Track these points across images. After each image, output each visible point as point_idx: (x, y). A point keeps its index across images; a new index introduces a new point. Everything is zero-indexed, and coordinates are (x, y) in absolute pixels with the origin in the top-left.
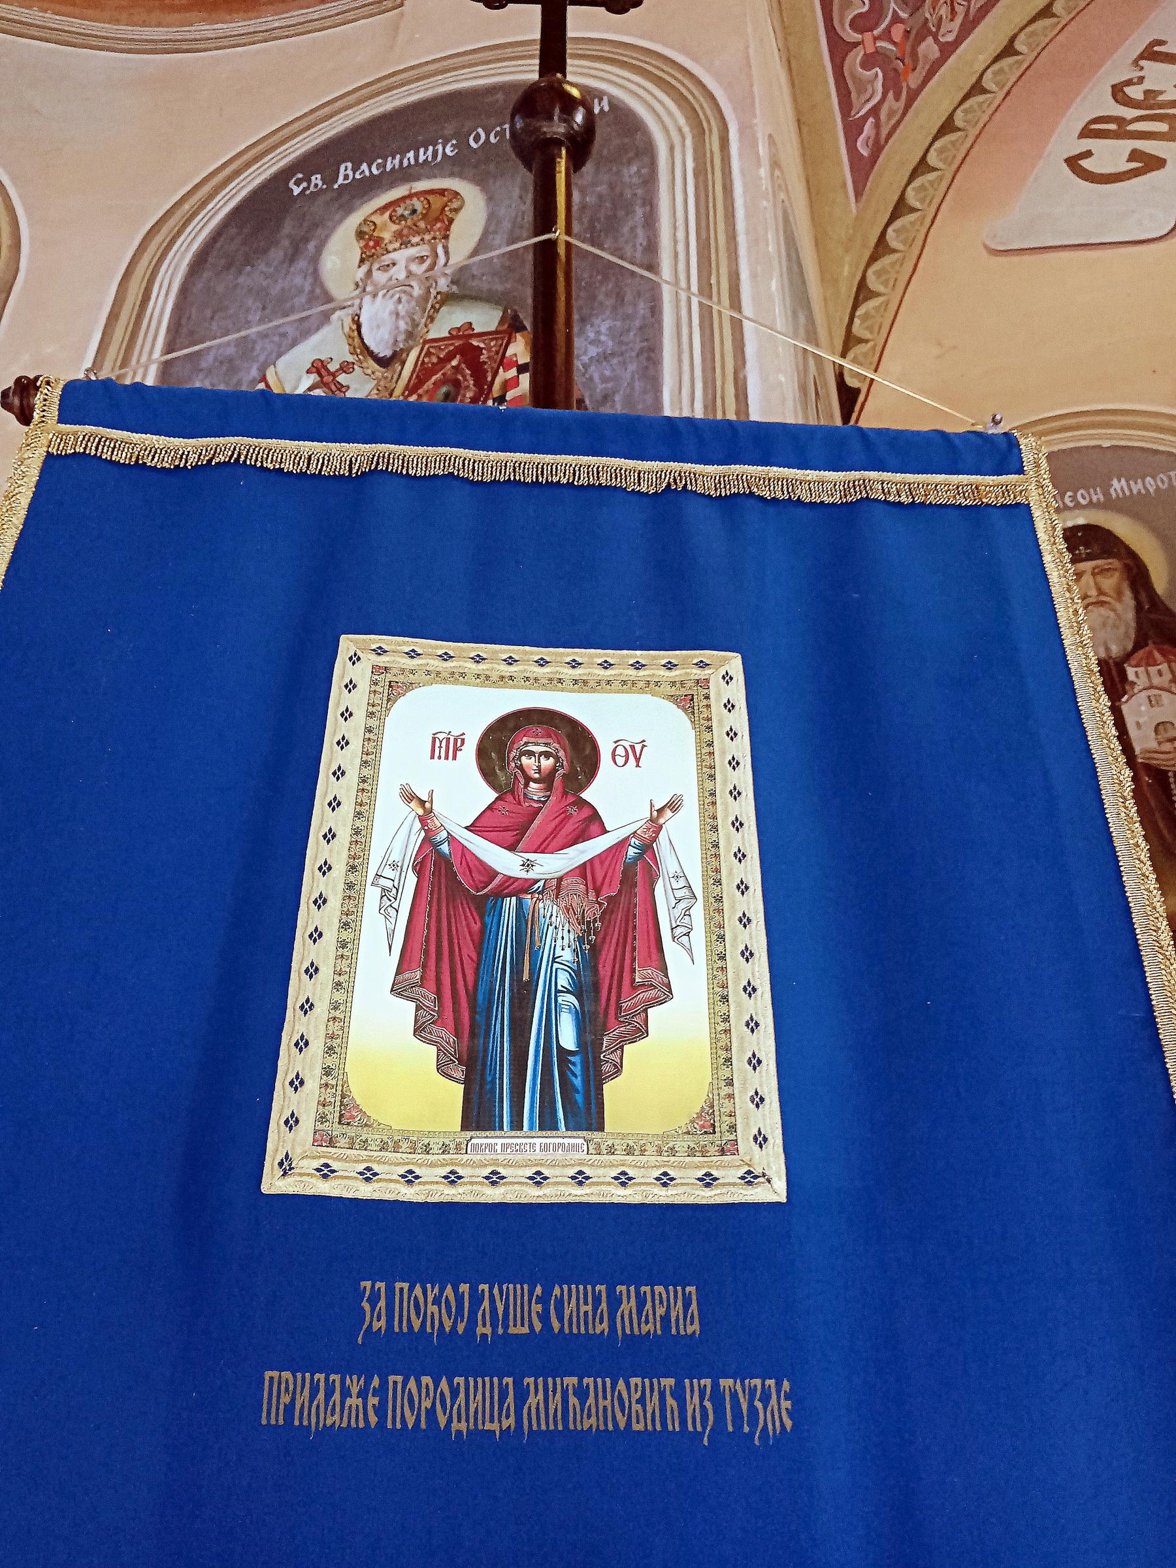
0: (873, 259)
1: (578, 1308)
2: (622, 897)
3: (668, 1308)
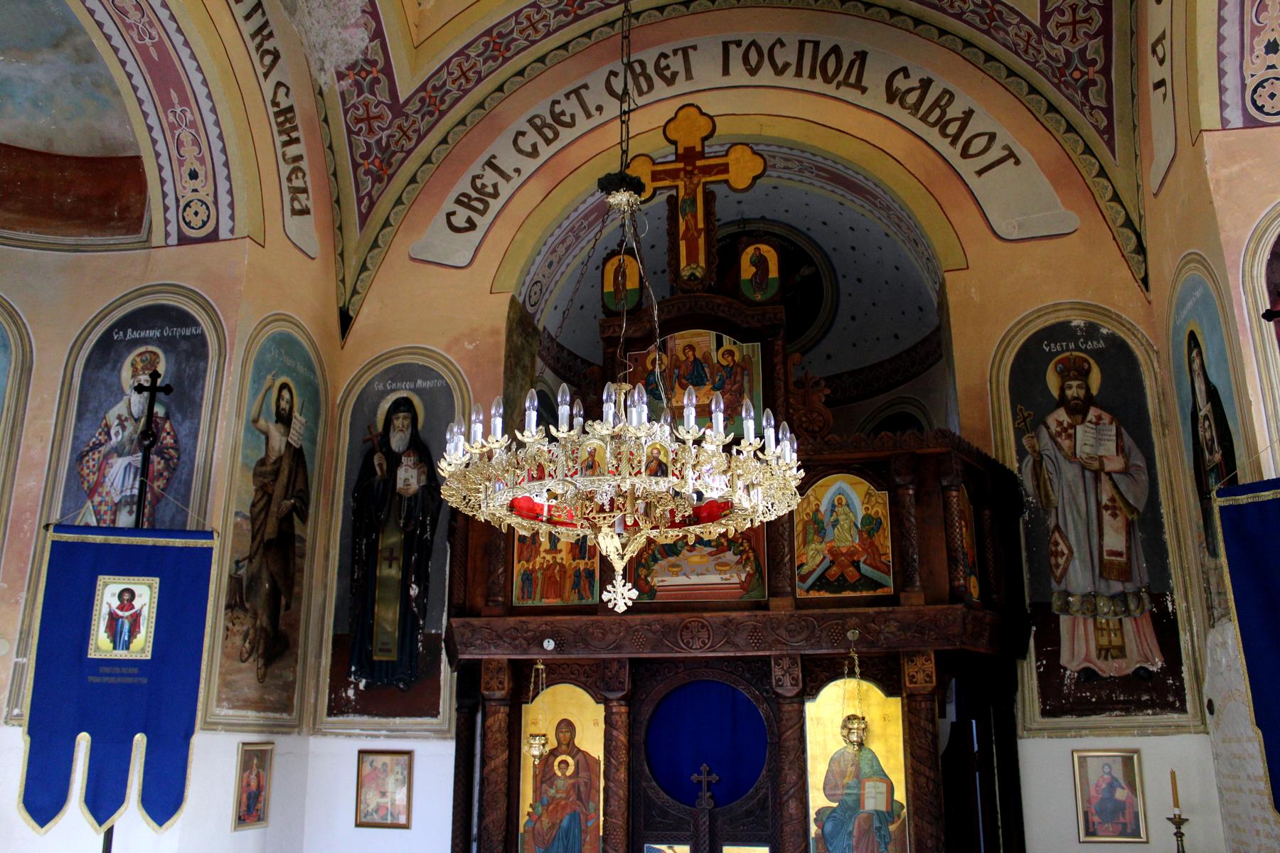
0: (371, 249)
1: (124, 670)
2: (135, 620)
3: (135, 670)
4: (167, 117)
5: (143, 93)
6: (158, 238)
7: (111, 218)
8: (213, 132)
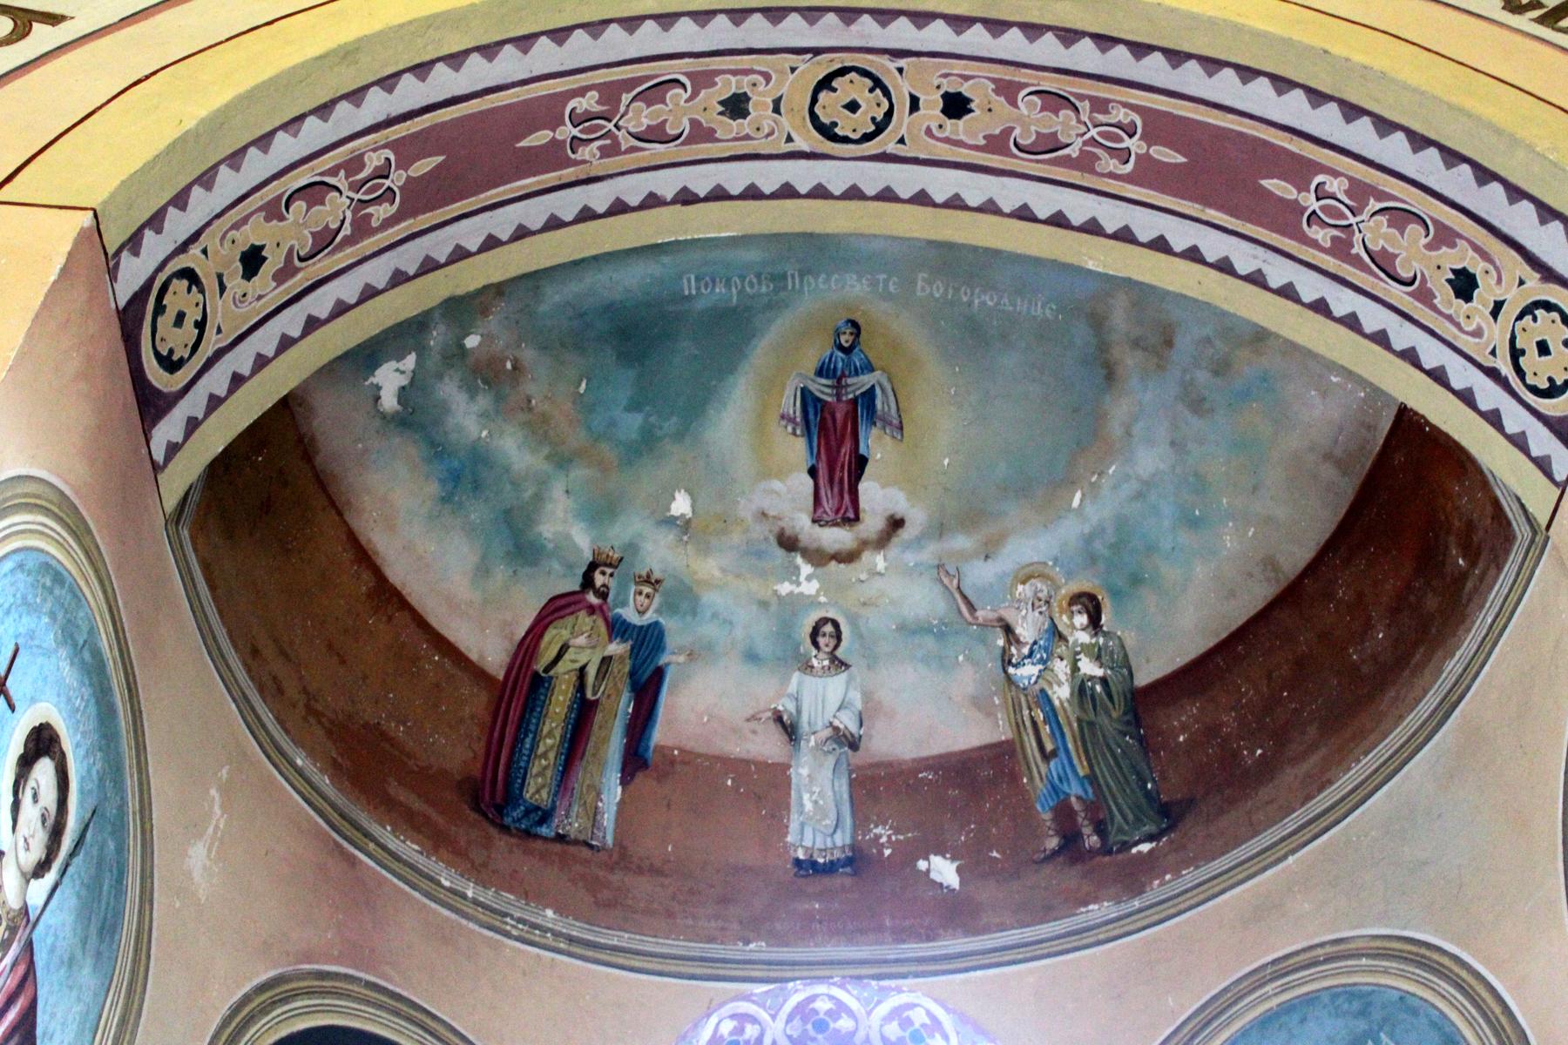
4: (1314, 244)
5: (1214, 245)
6: (1536, 495)
7: (1464, 576)
8: (1394, 150)
